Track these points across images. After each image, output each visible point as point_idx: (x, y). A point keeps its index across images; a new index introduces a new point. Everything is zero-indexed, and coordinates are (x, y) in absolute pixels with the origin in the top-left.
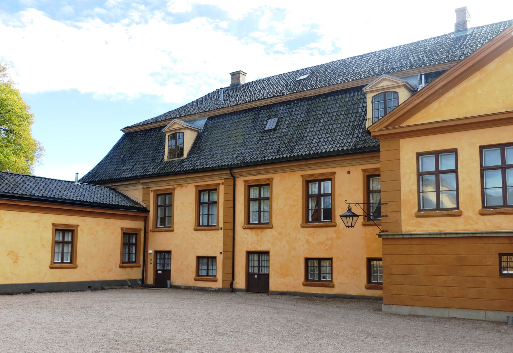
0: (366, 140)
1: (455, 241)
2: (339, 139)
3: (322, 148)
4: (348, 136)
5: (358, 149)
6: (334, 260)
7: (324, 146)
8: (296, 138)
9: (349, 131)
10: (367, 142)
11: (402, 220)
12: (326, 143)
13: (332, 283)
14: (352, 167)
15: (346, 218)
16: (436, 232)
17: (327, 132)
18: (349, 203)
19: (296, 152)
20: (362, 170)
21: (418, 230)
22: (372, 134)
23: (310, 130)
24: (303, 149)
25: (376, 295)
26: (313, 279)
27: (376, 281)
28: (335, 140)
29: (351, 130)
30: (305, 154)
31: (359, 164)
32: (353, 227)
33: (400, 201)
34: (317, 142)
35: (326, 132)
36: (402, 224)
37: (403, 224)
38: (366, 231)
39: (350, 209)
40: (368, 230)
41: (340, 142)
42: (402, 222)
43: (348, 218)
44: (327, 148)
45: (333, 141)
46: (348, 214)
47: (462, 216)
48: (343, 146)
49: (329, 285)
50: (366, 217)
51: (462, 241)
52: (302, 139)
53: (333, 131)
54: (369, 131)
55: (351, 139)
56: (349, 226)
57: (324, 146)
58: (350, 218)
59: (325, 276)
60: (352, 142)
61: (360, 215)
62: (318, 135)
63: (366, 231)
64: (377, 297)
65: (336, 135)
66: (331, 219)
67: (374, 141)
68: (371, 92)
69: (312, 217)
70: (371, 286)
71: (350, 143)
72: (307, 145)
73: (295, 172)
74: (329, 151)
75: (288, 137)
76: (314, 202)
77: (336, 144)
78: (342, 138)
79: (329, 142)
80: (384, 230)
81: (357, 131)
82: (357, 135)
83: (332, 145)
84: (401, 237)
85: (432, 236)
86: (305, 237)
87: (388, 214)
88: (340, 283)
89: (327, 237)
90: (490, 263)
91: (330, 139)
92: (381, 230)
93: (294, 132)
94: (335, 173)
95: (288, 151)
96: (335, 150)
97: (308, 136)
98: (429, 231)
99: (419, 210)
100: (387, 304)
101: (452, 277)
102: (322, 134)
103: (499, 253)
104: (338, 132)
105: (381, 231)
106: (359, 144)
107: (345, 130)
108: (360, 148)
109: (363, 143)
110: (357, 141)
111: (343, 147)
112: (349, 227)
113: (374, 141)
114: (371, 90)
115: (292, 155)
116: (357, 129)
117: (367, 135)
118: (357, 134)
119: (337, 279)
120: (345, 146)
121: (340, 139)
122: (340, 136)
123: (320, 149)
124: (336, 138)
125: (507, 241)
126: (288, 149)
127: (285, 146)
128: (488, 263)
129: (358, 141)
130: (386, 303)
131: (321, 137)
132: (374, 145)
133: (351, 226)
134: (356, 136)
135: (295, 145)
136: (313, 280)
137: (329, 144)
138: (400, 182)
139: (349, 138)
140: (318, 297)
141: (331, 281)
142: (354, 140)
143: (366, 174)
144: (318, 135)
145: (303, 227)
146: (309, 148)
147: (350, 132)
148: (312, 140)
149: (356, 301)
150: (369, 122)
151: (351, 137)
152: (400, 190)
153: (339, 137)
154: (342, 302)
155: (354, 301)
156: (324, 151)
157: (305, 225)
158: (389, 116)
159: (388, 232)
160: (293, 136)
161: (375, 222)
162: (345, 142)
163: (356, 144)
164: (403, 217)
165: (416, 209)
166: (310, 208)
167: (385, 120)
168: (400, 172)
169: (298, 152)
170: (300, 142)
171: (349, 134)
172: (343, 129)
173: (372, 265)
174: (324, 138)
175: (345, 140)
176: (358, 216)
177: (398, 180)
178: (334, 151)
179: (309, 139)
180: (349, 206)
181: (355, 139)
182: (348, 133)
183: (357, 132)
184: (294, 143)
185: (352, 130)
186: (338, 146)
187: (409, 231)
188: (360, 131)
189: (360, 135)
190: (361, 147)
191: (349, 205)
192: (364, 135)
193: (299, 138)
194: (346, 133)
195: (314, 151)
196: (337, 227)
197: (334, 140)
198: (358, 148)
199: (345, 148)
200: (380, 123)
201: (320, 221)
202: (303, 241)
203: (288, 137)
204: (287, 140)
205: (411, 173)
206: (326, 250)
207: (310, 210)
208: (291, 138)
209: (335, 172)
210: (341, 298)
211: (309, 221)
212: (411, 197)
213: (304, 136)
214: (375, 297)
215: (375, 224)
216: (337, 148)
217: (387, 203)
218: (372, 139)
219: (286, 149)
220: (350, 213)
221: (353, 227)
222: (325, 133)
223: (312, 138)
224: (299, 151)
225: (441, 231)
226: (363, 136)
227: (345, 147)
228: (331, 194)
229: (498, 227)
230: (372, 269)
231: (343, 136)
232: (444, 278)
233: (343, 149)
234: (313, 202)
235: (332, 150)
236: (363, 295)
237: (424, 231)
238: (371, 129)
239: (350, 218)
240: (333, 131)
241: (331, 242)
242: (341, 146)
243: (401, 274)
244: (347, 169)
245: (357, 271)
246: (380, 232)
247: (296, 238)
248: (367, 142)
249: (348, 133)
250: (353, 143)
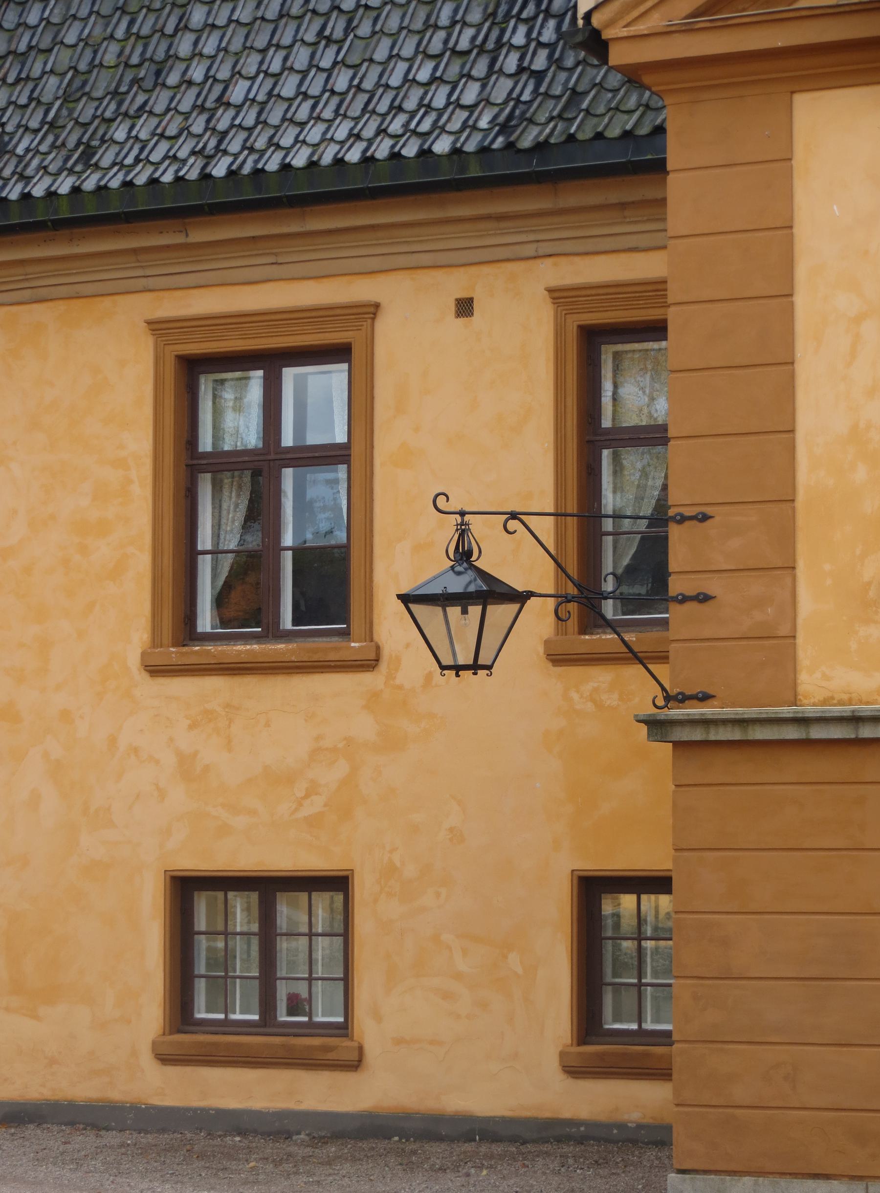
0: (576, 95)
2: (405, 80)
3: (286, 141)
4: (463, 66)
5: (520, 151)
6: (362, 889)
7: (302, 125)
8: (116, 66)
9: (469, 32)
10: (584, 106)
11: (800, 621)
12: (314, 107)
13: (345, 1043)
14: (486, 269)
15: (439, 610)
17: (327, 33)
18: (462, 514)
19: (114, 164)
20: (550, 291)
22: (618, 56)
23: (209, 13)
24: (163, 147)
25: (634, 1116)
26: (221, 1016)
27: (630, 1021)
28: (378, 85)
29: (479, 26)
30: (179, 179)
31: (530, 250)
32: (489, 668)
33: (793, 501)
34: (253, 100)
35: (320, 33)
36: (801, 654)
38: (575, 696)
39: (469, 553)
40: (587, 688)
41: (410, 104)
42: (800, 640)
43: (454, 612)
44: (323, 140)
45: (363, 98)
46: (456, 585)
48: (425, 126)
49: (331, 1056)
50: (573, 607)
52: (158, 73)
53: (365, 29)
54: (596, 34)
55: (484, 87)
56: (461, 661)
57: (302, 125)
58: (465, 612)
59: (304, 995)
60: (488, 102)
61: (530, 594)
62: (263, 51)
63: (575, 696)
64: (640, 1127)
65: (381, 54)
66: (346, 620)
67: (632, 102)
69: (220, 601)
71: (471, 108)
72: (187, 115)
73: (107, 302)
74: (339, 162)
75: (62, 58)
76: (237, 505)
77: (384, 116)
78: (423, 76)
79: (335, 100)
80: (688, 693)
81: (522, 30)
82: (522, 59)
83: (357, 120)
84: (792, 733)
86: (171, 740)
87: (712, 586)
88: (399, 1041)
89: (319, 738)
91: (341, 82)
92: (663, 689)
93: (107, 25)
94: (373, 310)
95: (64, 153)
96: (372, 158)
97: (198, 54)
102: (291, 46)
104: (394, 36)
105: (668, 698)
106: (531, 121)
107: (444, 20)
108: (541, 147)
109: (560, 116)
110: (518, 101)
111: (428, 133)
112: (458, 669)
113: (632, 102)
115: (89, 185)
116: (519, 19)
117: (584, 62)
118: (523, 50)
119: (378, 1017)
120: (438, 129)
121: (409, 81)
122: (411, 60)
123: (278, 146)
124: (381, 76)
126: (63, 144)
127: (43, 122)
129: (526, 97)
131: (283, 69)
132: (628, 127)
133: (475, 667)
134: (511, 63)
135: (108, 114)
136: (226, 1022)
137: (337, 112)
138: (792, 376)
139: (469, 76)
140: (256, 1132)
141: (344, 1029)
142: (501, 89)
144: (263, 51)
145: (155, 670)
146: (200, 136)
147: (474, 38)
148: (227, 84)
149: (501, 1157)
151: (480, 69)
152: (792, 431)
153: (402, 67)
154: (410, 1167)
155: (492, 1157)
156: (299, 160)
157: (174, 654)
159: (715, 702)
160: (95, 52)
161: (627, 637)
162: (439, 101)
163: (510, 116)
166: (205, 540)
168: (790, 310)
169: (129, 161)
170: (141, 99)
171: (468, 53)
172: (429, 16)
173: (610, 922)
174: (304, 74)
175: (444, 90)
176: (521, 598)
178: (367, 160)
179: (207, 77)
180: (463, 531)
181: (508, 83)
182: (464, 44)
183: (519, 39)
184: (101, 99)
185: (487, 25)
186: (396, 127)
187: (845, 697)
188: (540, 33)
189: (540, 62)
190: (546, 141)
192: (569, 62)
193: (139, 66)
194: (446, 42)
195: (236, 156)
196: (383, 666)
197: (368, 85)
198: (526, 142)
199: (442, 146)
201: (274, 633)
202: (157, 762)
203: (62, 58)
204: (53, 81)
205: (859, 319)
206: (313, 822)
207: (209, 557)
208: (83, 66)
209: (377, 306)
210: (405, 1135)
211: (200, 629)
213: (171, 57)
214: (622, 1126)
215: (631, 650)
216: (387, 143)
217: (708, 510)
218: (616, 91)
219: (50, 138)
220: (470, 575)
221: (489, 668)
222: (310, 37)
223: (224, 74)
224: (137, 160)
226: (561, 68)
227: (444, 136)
228: (347, 446)
230: (608, 946)
231: (429, 65)
233: (430, 151)
234: (225, 506)
235: (353, 156)
236: (547, 1114)
238: (611, 23)
239: (465, 612)
240: (365, 29)
241: (342, 769)
242: (414, 132)
245: (514, 960)
246: (660, 702)
247: (113, 741)
248: (584, 106)
249: (464, 44)
250: (496, 110)
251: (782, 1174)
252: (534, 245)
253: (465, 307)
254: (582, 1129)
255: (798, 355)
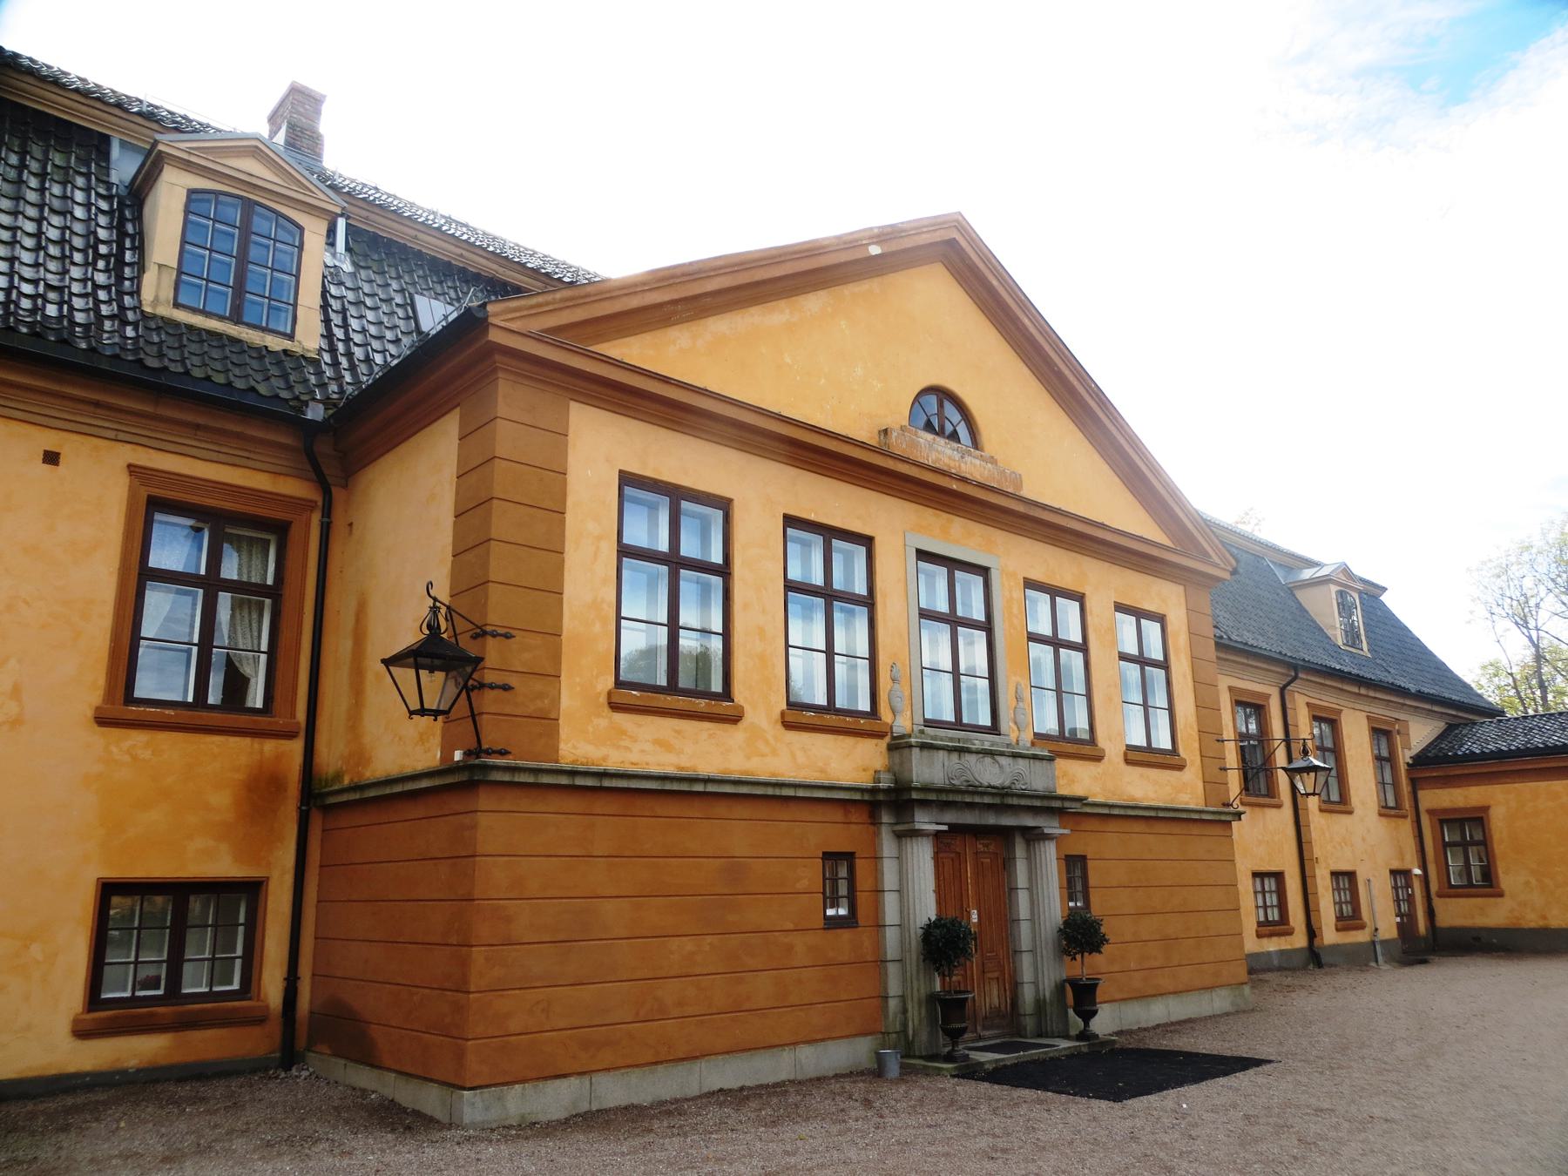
1: (721, 809)
16: (670, 770)
21: (614, 759)
25: (132, 1063)
37: (565, 731)
38: (114, 749)
40: (127, 744)
42: (561, 721)
47: (740, 725)
51: (741, 810)
63: (114, 749)
64: (139, 1071)
68: (188, 166)
70: (110, 1019)
80: (495, 749)
84: (564, 780)
85: (668, 786)
87: (512, 680)
90: (802, 885)
98: (647, 764)
99: (619, 684)
100: (480, 1087)
101: (709, 939)
103: (823, 853)
114: (193, 159)
125: (837, 815)
128: (800, 886)
130: (475, 1084)
143: (144, 493)
150: (159, 279)
158: (567, 300)
164: (565, 702)
165: (610, 682)
167: (551, 307)
177: (555, 551)
191: (434, 606)
200: (532, 307)
205: (599, 538)
212: (597, 628)
225: (682, 769)
229: (822, 771)
232: (689, 945)
237: (632, 764)
238: (496, 315)
243: (548, 940)
244: (50, 440)
245: (36, 951)
251: (538, 1079)
252: (115, 433)
253: (51, 458)
254: (88, 1079)
255: (566, 549)
